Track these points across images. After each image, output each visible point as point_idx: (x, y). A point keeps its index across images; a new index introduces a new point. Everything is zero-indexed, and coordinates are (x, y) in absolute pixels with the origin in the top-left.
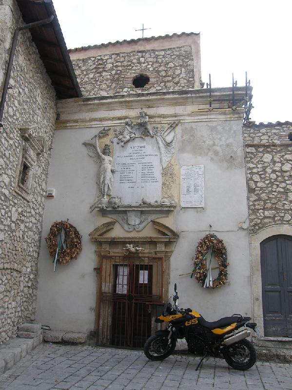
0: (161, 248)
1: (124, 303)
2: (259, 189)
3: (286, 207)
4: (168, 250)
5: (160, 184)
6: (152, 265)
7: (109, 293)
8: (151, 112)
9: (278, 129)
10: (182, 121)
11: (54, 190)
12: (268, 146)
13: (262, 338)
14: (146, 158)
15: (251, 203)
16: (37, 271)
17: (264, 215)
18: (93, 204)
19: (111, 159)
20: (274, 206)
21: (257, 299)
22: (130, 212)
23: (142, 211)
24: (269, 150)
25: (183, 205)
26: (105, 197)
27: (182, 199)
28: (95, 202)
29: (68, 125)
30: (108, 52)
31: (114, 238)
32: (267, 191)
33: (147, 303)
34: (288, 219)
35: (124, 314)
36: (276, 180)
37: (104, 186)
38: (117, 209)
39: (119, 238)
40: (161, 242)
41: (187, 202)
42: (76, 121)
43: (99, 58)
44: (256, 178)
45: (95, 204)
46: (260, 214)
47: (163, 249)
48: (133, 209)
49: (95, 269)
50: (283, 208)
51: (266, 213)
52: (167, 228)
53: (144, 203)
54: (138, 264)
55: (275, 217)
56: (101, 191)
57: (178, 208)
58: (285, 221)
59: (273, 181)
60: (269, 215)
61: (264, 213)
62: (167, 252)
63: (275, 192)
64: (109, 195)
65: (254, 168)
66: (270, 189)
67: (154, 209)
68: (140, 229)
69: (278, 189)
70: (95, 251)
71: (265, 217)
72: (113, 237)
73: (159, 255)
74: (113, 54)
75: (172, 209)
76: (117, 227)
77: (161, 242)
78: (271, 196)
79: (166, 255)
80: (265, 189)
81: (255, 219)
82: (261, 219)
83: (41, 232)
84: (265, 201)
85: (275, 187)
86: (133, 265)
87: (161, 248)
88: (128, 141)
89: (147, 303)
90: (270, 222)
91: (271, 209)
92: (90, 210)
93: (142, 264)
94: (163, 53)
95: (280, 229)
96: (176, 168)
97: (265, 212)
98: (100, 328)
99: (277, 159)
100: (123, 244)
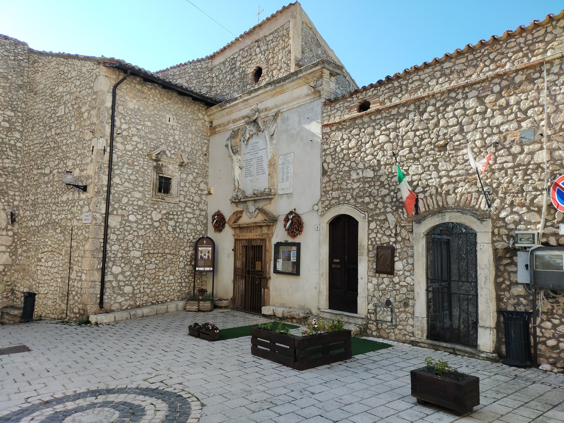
0: (265, 230)
5: (267, 174)
6: (262, 246)
8: (261, 106)
9: (350, 102)
10: (281, 111)
12: (339, 123)
14: (259, 152)
15: (324, 185)
19: (240, 157)
24: (340, 127)
25: (280, 192)
29: (216, 130)
30: (236, 49)
36: (343, 158)
39: (244, 224)
41: (283, 189)
42: (220, 126)
43: (232, 57)
44: (329, 159)
55: (340, 197)
59: (340, 160)
65: (328, 149)
66: (338, 169)
74: (240, 51)
75: (272, 197)
78: (337, 176)
82: (330, 201)
85: (342, 166)
87: (265, 230)
88: (249, 138)
91: (337, 190)
94: (271, 37)
96: (276, 158)
99: (345, 137)
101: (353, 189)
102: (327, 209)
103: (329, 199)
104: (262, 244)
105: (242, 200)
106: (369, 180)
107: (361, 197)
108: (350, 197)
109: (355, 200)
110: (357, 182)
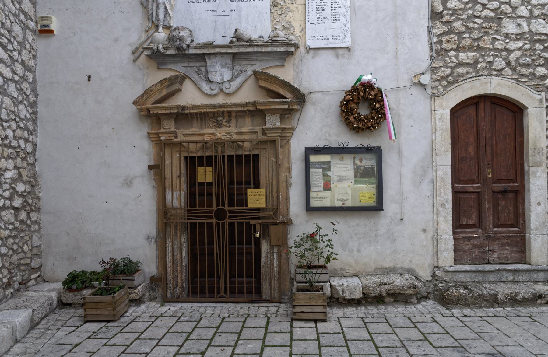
0: (274, 122)
1: (210, 225)
2: (451, 12)
3: (498, 45)
4: (287, 127)
6: (257, 157)
7: (181, 208)
11: (54, 19)
13: (452, 269)
16: (35, 176)
17: (457, 59)
18: (137, 45)
20: (476, 44)
21: (443, 205)
22: (212, 56)
23: (234, 55)
25: (312, 43)
26: (161, 29)
27: (308, 33)
28: (142, 41)
31: (184, 108)
32: (464, 17)
33: (252, 222)
34: (500, 67)
35: (211, 243)
37: (158, 8)
38: (187, 52)
40: (273, 112)
45: (141, 44)
46: (450, 58)
47: (278, 124)
48: (218, 50)
49: (150, 167)
50: (491, 47)
51: (463, 56)
52: (286, 85)
53: (239, 38)
54: (233, 153)
55: (476, 62)
56: (149, 17)
57: (302, 50)
58: (495, 70)
60: (468, 61)
61: (457, 57)
62: (284, 129)
63: (479, 17)
64: (168, 27)
66: (470, 12)
67: (259, 49)
68: (231, 90)
69: (486, 13)
70: (149, 134)
71: (461, 64)
72: (182, 104)
73: (271, 135)
75: (293, 49)
76: (188, 86)
77: (273, 112)
78: (471, 25)
79: (284, 135)
80: (460, 12)
81: (441, 67)
82: (452, 68)
83: (35, 102)
84: (460, 34)
86: (223, 156)
87: (274, 122)
89: (252, 222)
90: (468, 73)
91: (470, 49)
92: (133, 57)
93: (240, 152)
95: (486, 83)
97: (461, 54)
98: (169, 269)
100: (201, 118)
101: (509, 51)
102: (444, 83)
103: (451, 65)
104: (256, 152)
105: (191, 51)
106: (543, 37)
107: (527, 66)
108: (503, 64)
109: (514, 70)
110: (518, 40)
